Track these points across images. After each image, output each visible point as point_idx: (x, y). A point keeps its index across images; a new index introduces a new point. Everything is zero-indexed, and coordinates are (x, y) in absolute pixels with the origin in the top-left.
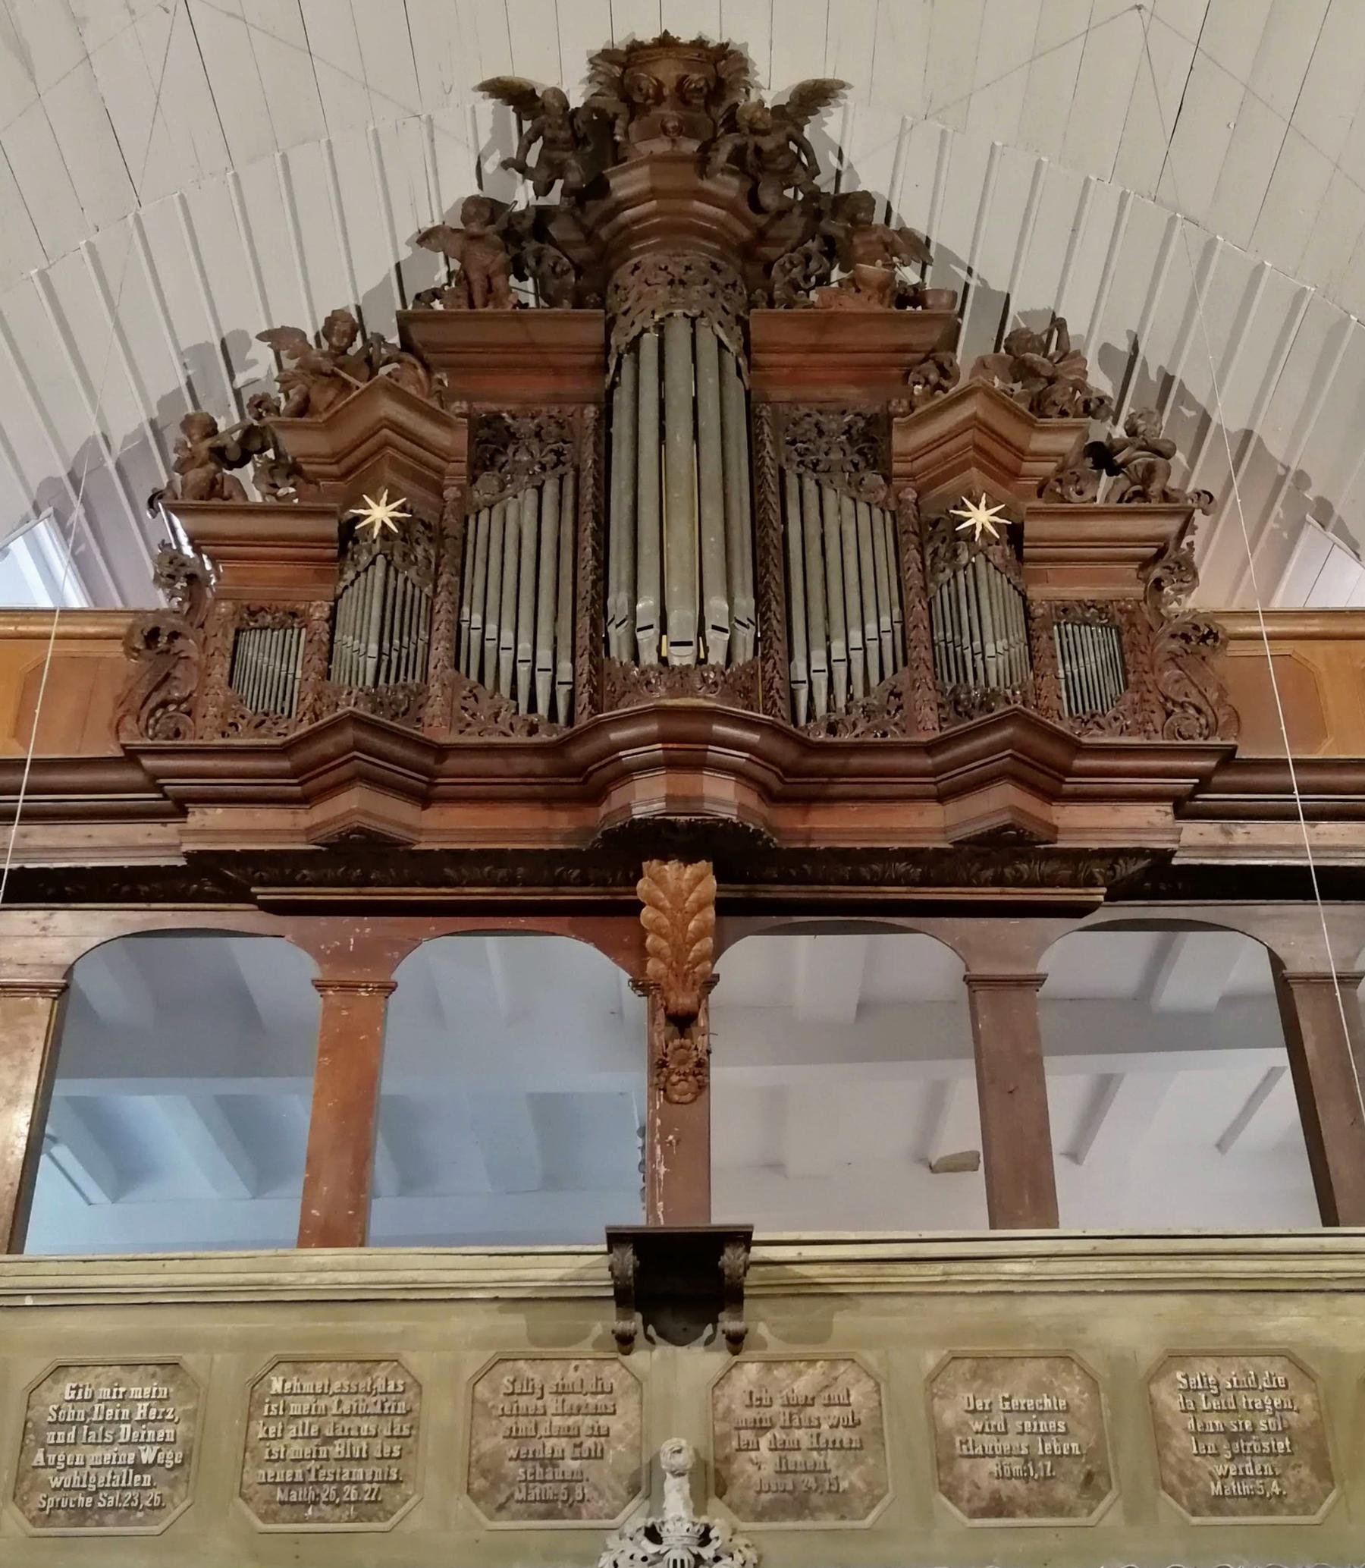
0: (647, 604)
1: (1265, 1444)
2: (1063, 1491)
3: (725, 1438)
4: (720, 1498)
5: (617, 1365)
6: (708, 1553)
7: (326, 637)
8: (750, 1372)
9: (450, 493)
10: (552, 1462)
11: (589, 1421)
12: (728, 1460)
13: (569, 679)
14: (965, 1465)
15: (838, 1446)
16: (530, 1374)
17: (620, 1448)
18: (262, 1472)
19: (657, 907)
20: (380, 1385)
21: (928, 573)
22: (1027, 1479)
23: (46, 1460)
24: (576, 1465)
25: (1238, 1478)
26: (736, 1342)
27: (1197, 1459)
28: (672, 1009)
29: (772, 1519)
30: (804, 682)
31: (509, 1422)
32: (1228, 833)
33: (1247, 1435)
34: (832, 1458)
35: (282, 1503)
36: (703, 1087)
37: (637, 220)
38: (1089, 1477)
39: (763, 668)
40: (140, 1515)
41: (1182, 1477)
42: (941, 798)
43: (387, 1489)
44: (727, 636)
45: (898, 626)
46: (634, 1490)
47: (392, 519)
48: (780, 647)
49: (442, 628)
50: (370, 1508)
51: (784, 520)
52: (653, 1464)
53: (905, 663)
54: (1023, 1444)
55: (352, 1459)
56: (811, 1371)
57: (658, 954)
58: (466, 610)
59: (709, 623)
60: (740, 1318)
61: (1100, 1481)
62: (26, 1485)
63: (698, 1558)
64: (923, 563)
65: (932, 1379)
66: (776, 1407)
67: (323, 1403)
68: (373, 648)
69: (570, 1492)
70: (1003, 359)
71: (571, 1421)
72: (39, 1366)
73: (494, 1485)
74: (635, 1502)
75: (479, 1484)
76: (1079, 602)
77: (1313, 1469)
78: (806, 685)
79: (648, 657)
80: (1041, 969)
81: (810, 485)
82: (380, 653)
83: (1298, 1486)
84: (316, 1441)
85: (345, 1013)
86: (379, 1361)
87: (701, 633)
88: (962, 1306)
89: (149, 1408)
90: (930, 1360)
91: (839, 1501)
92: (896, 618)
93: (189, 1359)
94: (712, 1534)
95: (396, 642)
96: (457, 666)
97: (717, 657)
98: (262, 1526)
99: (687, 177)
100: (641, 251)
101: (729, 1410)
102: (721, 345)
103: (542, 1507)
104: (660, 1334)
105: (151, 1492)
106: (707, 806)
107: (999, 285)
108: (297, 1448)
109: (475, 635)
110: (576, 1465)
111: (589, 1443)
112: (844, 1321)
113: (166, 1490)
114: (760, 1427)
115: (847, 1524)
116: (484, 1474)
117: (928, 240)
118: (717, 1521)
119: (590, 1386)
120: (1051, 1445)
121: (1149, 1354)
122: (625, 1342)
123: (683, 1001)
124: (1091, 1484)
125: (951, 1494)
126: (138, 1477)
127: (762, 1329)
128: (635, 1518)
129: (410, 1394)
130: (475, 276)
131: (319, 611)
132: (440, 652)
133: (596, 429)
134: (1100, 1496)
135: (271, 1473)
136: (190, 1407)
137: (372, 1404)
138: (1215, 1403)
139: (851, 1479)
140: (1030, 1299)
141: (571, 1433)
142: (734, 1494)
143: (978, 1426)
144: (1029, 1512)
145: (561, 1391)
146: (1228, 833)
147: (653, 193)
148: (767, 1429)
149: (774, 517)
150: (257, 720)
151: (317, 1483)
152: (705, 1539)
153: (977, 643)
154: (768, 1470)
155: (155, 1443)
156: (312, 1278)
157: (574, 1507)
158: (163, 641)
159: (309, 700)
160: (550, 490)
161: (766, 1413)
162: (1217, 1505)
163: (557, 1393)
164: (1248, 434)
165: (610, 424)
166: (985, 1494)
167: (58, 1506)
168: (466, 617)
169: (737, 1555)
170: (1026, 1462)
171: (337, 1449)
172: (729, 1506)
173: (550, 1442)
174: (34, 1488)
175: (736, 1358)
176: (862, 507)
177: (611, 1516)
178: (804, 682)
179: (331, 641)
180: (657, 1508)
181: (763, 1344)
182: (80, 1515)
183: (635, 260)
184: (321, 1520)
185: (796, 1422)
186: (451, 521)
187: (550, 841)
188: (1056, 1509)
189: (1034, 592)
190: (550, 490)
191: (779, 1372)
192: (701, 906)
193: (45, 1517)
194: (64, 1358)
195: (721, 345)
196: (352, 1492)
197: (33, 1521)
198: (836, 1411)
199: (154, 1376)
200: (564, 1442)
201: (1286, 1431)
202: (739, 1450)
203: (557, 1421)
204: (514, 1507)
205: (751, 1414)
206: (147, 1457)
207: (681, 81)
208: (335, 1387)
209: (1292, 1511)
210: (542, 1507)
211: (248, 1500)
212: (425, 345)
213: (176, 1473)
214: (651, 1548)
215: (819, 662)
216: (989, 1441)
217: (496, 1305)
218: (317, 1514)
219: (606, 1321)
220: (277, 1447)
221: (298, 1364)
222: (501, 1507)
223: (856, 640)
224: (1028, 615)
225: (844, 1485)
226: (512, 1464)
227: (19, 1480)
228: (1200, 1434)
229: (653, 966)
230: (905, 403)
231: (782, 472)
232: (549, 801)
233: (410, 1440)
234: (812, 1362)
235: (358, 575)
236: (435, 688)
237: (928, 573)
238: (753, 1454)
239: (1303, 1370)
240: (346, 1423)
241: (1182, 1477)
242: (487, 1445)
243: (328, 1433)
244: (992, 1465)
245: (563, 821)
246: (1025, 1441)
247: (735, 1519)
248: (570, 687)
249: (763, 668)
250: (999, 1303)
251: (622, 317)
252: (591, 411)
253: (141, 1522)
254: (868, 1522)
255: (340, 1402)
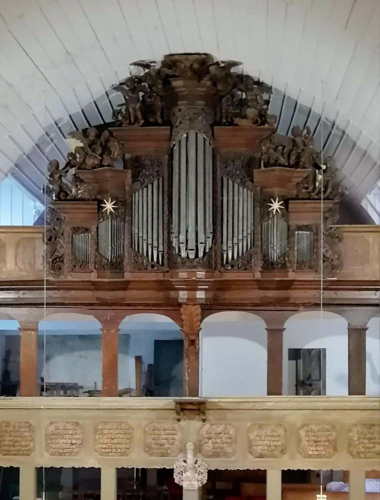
0: (182, 238)
1: (323, 443)
2: (277, 453)
3: (201, 441)
4: (200, 453)
5: (177, 424)
6: (197, 466)
7: (96, 238)
8: (207, 426)
9: (127, 188)
10: (163, 445)
11: (171, 436)
12: (201, 445)
13: (162, 250)
14: (255, 447)
15: (226, 443)
16: (157, 426)
17: (178, 442)
18: (99, 446)
19: (186, 315)
20: (123, 427)
21: (262, 218)
22: (268, 450)
23: (51, 442)
24: (168, 446)
25: (316, 451)
26: (204, 421)
27: (307, 446)
28: (190, 339)
29: (211, 458)
30: (225, 251)
31: (153, 436)
32: (336, 294)
33: (319, 441)
34: (225, 445)
35: (104, 452)
36: (198, 358)
37: (181, 92)
38: (282, 450)
39: (215, 247)
40: (73, 454)
41: (303, 451)
42: (260, 289)
43: (127, 450)
44: (204, 245)
45: (252, 232)
46: (181, 451)
47: (111, 202)
48: (219, 240)
49: (127, 235)
50: (122, 454)
51: (222, 196)
52: (185, 446)
53: (253, 246)
54: (268, 443)
55: (119, 443)
56: (221, 426)
57: (186, 325)
58: (133, 227)
59: (199, 242)
60: (205, 416)
61: (285, 451)
62: (48, 447)
63: (195, 467)
64: (261, 212)
65: (248, 429)
66: (213, 434)
67: (111, 431)
68: (110, 247)
69: (167, 451)
70: (289, 138)
71: (167, 436)
72: (48, 422)
73: (150, 450)
74: (180, 454)
75: (147, 449)
76: (303, 226)
77: (333, 448)
78: (226, 252)
79: (183, 254)
80: (284, 327)
81: (230, 183)
82: (112, 248)
83: (329, 453)
84: (110, 439)
85: (108, 337)
86: (123, 422)
87: (197, 246)
88: (258, 412)
89: (73, 431)
90: (249, 424)
91: (226, 455)
92: (252, 229)
93: (80, 422)
94: (198, 462)
95: (116, 243)
96: (132, 247)
97: (201, 254)
98: (100, 457)
99: (196, 82)
100: (182, 105)
101: (202, 435)
102: (204, 139)
103: (161, 454)
104: (187, 418)
105: (75, 449)
106: (199, 301)
107: (294, 97)
108: (106, 441)
109: (136, 235)
110: (168, 446)
111: (171, 441)
112: (229, 415)
113: (78, 449)
114: (209, 439)
115: (227, 459)
116: (148, 447)
117: (271, 87)
118: (199, 458)
119: (171, 428)
120: (275, 443)
121: (299, 424)
122: (179, 420)
123: (193, 337)
124: (283, 452)
125: (251, 454)
126: (72, 446)
127: (210, 417)
128: (181, 457)
129: (131, 430)
130: (131, 110)
131: (94, 229)
132: (127, 242)
133: (168, 164)
134: (284, 454)
135: (101, 446)
136: (81, 431)
137: (122, 432)
138: (313, 434)
139: (229, 450)
140: (273, 411)
141: (167, 439)
142: (203, 452)
143: (258, 439)
144: (268, 457)
145: (164, 430)
146: (336, 294)
147: (184, 86)
148: (211, 439)
149: (219, 196)
150: (80, 264)
151: (111, 448)
152: (196, 463)
153: (272, 245)
154: (211, 447)
155: (75, 439)
156: (106, 404)
157: (168, 455)
158: (53, 240)
159: (94, 258)
160: (155, 184)
161: (210, 435)
162: (310, 456)
163: (163, 430)
164: (366, 152)
165: (172, 160)
166: (259, 453)
167: (55, 452)
168: (133, 230)
169: (203, 466)
170: (268, 447)
171: (115, 441)
172: (202, 455)
173: (162, 441)
174: (49, 448)
175: (204, 423)
176: (245, 190)
177: (176, 456)
178: (225, 251)
179: (98, 239)
180: (186, 456)
181: (210, 421)
182: (61, 454)
183: (179, 107)
184: (113, 456)
185: (217, 438)
186: (127, 197)
187: (158, 301)
188: (274, 457)
189: (290, 223)
190: (155, 184)
191: (214, 427)
192: (197, 315)
193: (53, 454)
194: (52, 420)
195: (204, 139)
196: (119, 450)
197: (51, 455)
198: (226, 435)
199: (73, 424)
200: (165, 441)
201: (328, 440)
202: (204, 443)
203: (164, 436)
204: (155, 454)
205: (207, 436)
206: (74, 442)
207: (192, 65)
208: (114, 428)
209: (327, 458)
210: (161, 454)
211: (96, 451)
212: (117, 136)
213: (81, 445)
214: (185, 464)
215: (230, 244)
216: (260, 442)
217: (149, 410)
218: (112, 455)
219: (173, 415)
220: (102, 441)
221: (105, 423)
222: (151, 454)
223: (240, 238)
224: (289, 229)
225: (227, 451)
226: (154, 445)
227: (46, 446)
228: (308, 441)
229: (185, 328)
230: (260, 154)
231: (222, 179)
232: (158, 290)
233: (131, 440)
234: (221, 425)
235: (104, 220)
236: (126, 254)
237: (262, 218)
238: (207, 444)
239: (334, 427)
240: (117, 436)
241: (303, 451)
242: (148, 441)
243: (113, 438)
244: (261, 447)
245: (161, 294)
246: (269, 442)
247: (203, 458)
248: (162, 253)
249: (215, 247)
250: (266, 412)
251: (175, 128)
252: (166, 157)
253: (74, 456)
254: (232, 459)
255: (115, 431)
